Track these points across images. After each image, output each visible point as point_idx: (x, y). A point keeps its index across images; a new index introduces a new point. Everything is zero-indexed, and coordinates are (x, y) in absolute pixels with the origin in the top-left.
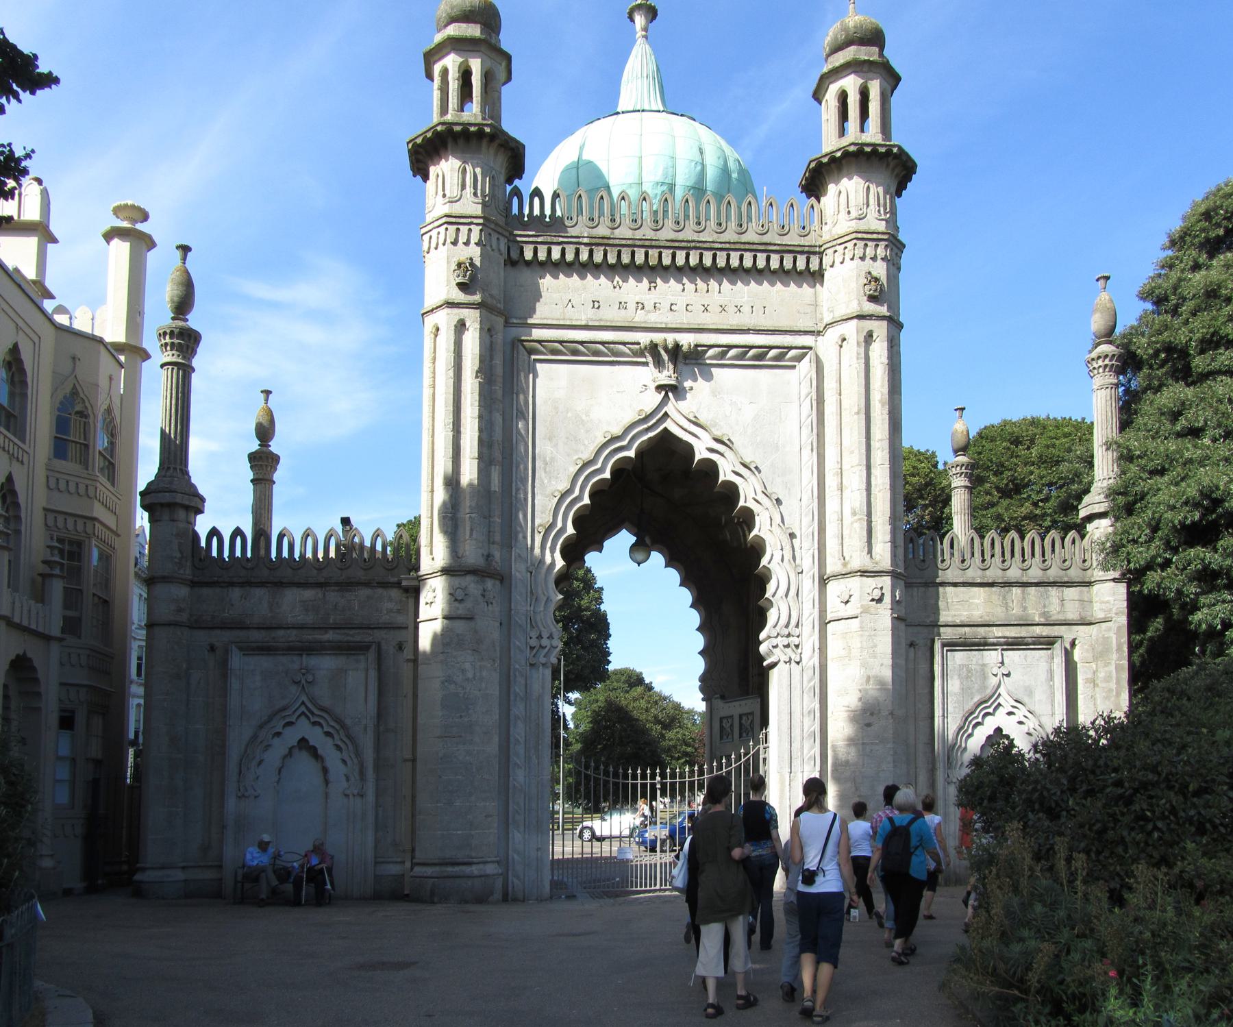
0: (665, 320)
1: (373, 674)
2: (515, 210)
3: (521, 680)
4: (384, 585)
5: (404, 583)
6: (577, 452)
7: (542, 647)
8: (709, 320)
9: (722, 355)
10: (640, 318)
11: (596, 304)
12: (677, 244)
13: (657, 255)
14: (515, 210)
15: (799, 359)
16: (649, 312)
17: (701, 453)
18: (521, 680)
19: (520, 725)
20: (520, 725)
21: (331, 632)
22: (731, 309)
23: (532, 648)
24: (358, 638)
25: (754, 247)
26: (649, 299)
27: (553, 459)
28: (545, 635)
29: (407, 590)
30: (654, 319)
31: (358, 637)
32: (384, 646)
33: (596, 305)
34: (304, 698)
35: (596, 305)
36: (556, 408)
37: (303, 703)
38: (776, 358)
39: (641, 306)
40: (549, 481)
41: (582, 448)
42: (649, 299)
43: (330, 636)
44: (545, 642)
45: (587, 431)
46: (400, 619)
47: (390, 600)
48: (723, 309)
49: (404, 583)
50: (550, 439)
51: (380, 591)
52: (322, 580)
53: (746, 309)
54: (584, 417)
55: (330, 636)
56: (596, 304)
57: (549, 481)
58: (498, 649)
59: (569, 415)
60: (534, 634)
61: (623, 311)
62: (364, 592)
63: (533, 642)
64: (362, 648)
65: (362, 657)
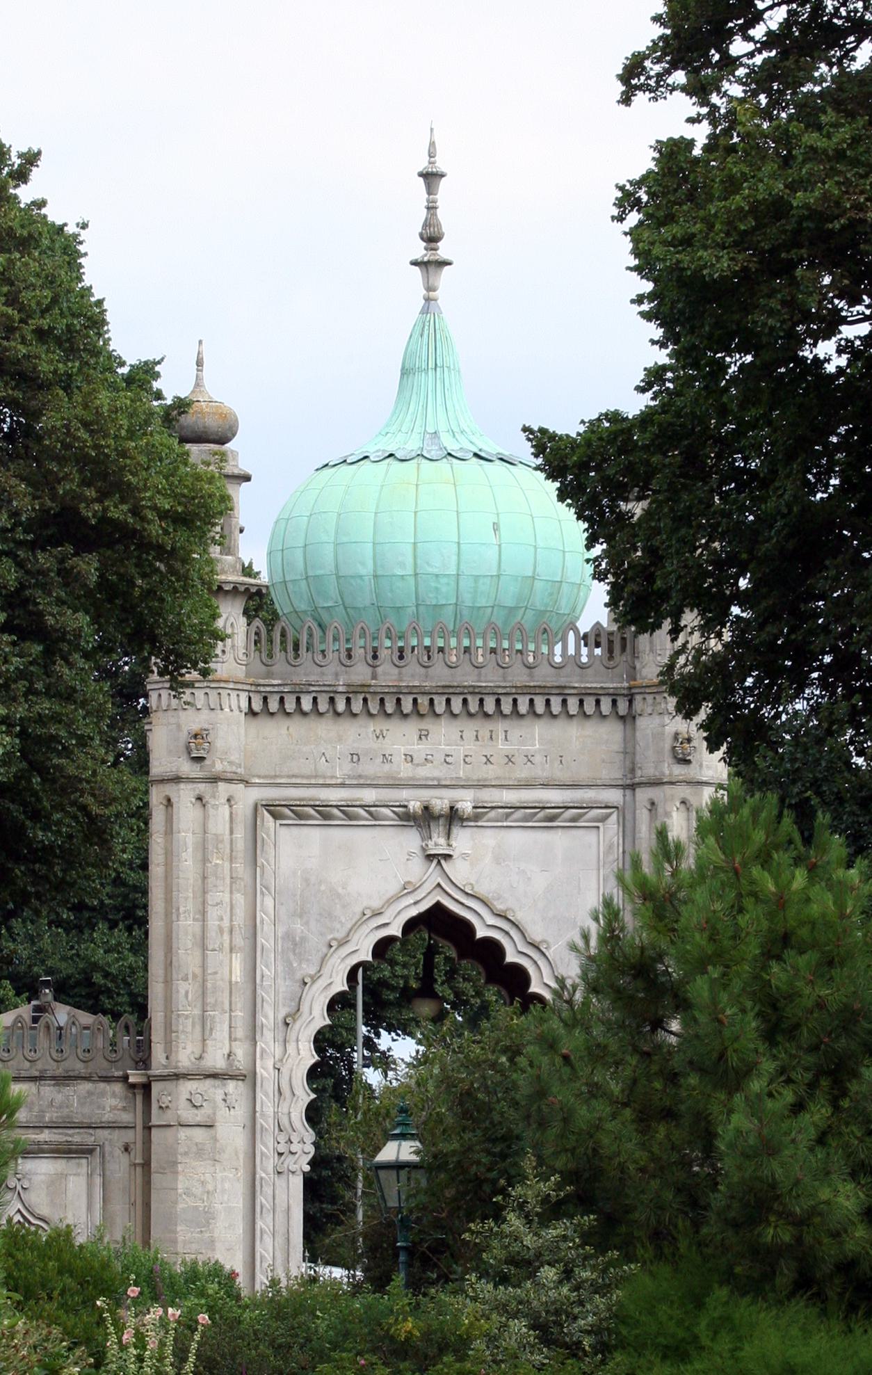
0: (436, 774)
1: (98, 1180)
3: (268, 1190)
4: (107, 1079)
5: (131, 1080)
6: (332, 930)
7: (291, 1153)
8: (490, 772)
9: (508, 816)
10: (405, 771)
11: (355, 757)
12: (451, 690)
13: (426, 703)
15: (603, 819)
16: (418, 765)
17: (481, 933)
18: (268, 1190)
19: (268, 1240)
20: (268, 1240)
21: (47, 1131)
22: (520, 760)
23: (280, 1154)
24: (77, 1139)
25: (546, 691)
26: (420, 749)
27: (303, 939)
28: (295, 1139)
29: (133, 1086)
30: (424, 772)
31: (77, 1137)
32: (107, 1149)
33: (355, 758)
34: (20, 1206)
35: (355, 758)
36: (307, 881)
37: (19, 1211)
38: (574, 820)
39: (409, 758)
40: (300, 964)
41: (338, 926)
42: (420, 749)
43: (45, 1136)
44: (294, 1148)
45: (344, 907)
46: (126, 1118)
47: (114, 1095)
48: (509, 759)
49: (131, 1080)
50: (301, 916)
51: (102, 1085)
52: (37, 1074)
53: (538, 759)
54: (340, 890)
55: (45, 1136)
56: (355, 757)
57: (300, 964)
58: (241, 1156)
59: (323, 888)
60: (282, 1138)
61: (387, 767)
62: (85, 1087)
63: (281, 1149)
64: (84, 1151)
65: (84, 1161)
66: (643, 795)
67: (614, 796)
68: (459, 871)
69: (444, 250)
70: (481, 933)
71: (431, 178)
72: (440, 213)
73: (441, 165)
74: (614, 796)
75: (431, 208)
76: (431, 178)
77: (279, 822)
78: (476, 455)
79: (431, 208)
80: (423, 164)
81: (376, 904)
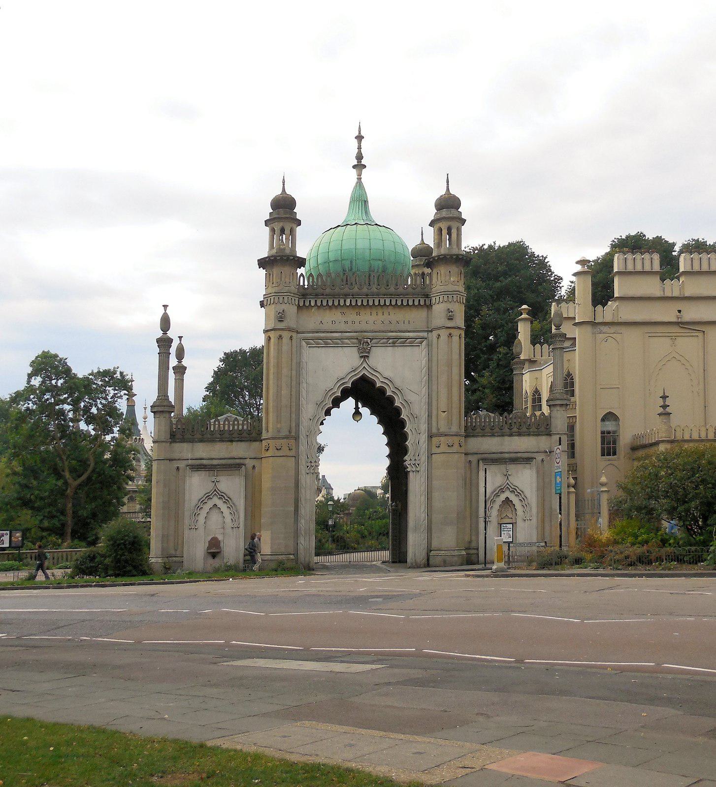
2: (302, 284)
14: (302, 284)
17: (378, 385)
39: (353, 322)
42: (358, 319)
66: (435, 333)
67: (425, 334)
68: (372, 361)
69: (363, 162)
70: (378, 385)
71: (360, 138)
72: (362, 150)
73: (362, 134)
74: (425, 334)
75: (359, 148)
76: (360, 138)
77: (308, 346)
78: (376, 224)
79: (359, 148)
80: (357, 134)
81: (342, 375)
